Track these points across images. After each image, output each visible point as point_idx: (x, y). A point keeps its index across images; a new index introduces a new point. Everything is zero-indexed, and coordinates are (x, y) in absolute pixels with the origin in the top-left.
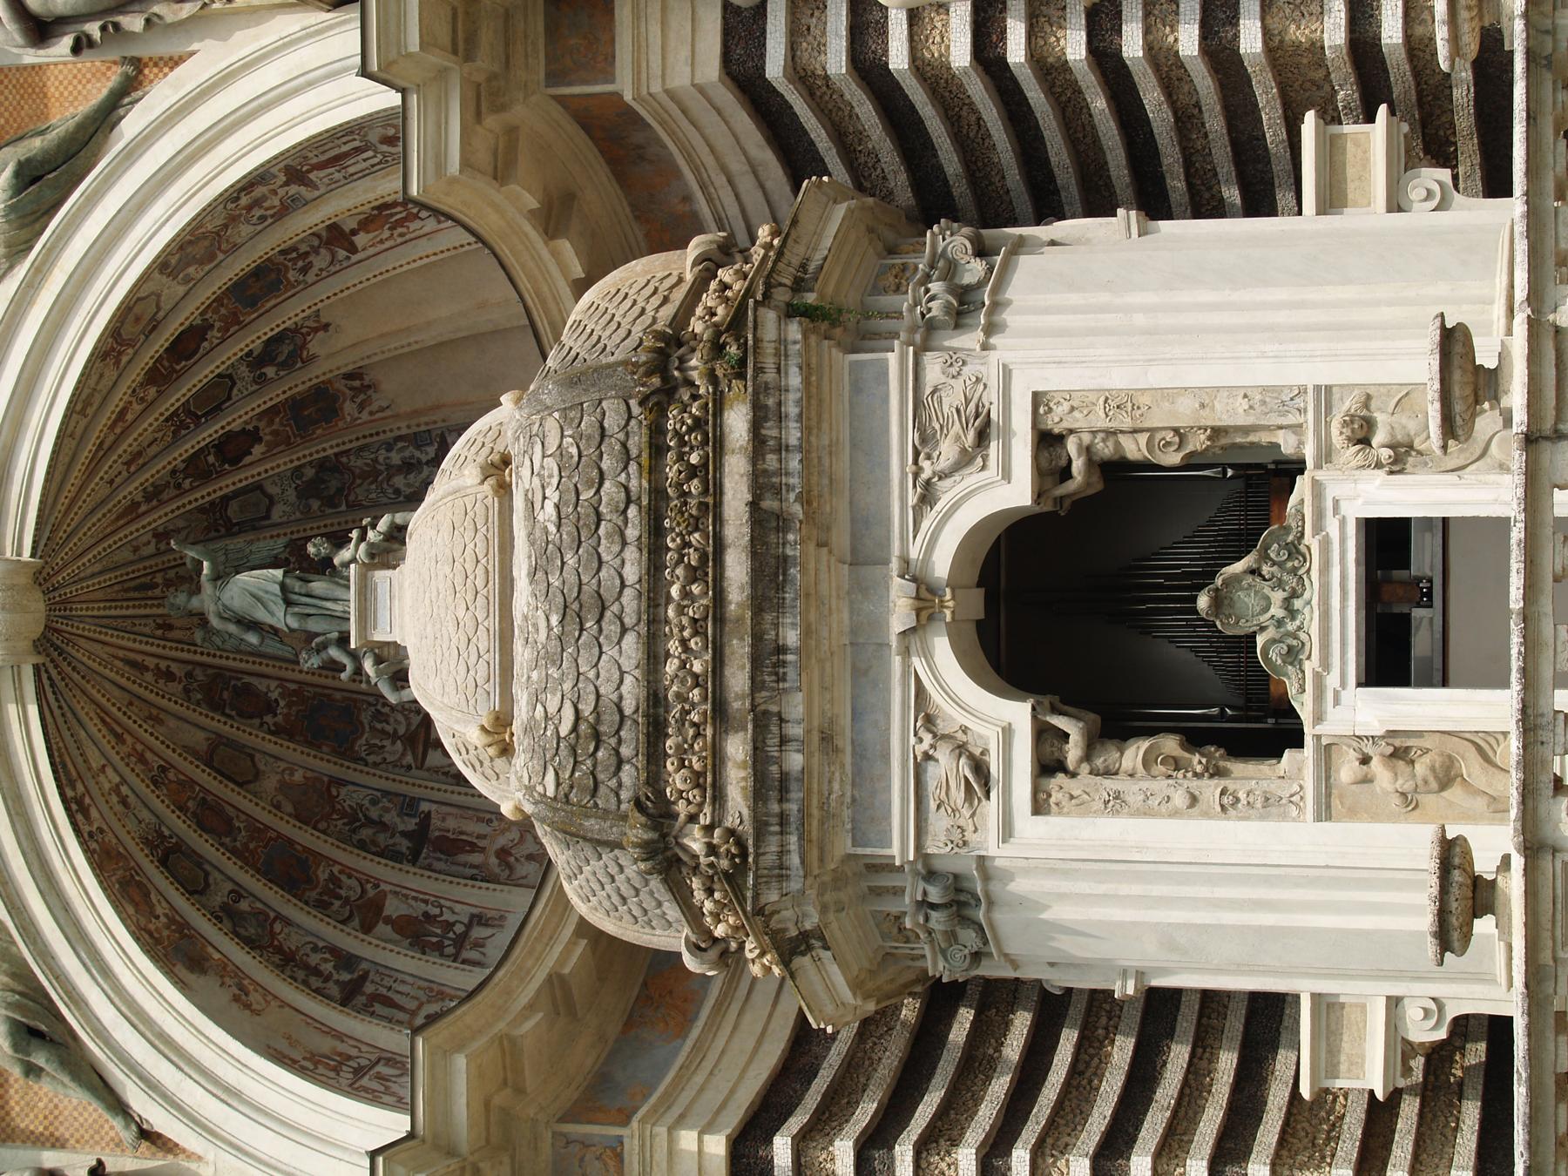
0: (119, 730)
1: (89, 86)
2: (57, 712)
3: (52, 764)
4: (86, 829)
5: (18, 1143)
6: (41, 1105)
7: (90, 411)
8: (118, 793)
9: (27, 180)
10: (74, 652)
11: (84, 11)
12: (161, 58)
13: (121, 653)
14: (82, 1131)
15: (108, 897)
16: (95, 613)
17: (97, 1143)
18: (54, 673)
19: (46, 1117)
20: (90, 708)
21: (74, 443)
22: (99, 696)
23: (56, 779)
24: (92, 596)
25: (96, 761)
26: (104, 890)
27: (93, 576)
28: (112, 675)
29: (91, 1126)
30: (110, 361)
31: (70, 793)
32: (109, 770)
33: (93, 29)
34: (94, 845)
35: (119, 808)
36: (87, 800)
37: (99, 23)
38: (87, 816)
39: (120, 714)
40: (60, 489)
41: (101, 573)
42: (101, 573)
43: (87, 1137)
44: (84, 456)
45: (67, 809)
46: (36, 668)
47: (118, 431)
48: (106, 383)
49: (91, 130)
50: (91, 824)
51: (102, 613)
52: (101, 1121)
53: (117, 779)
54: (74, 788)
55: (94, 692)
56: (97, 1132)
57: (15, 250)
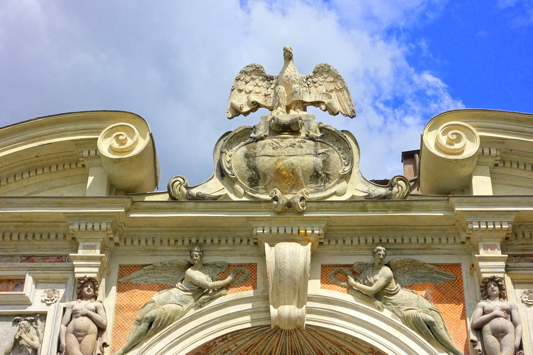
0: (249, 350)
2: (255, 332)
3: (238, 331)
4: (217, 341)
5: (114, 316)
6: (127, 324)
7: (354, 343)
8: (228, 350)
9: (429, 325)
10: (275, 336)
11: (485, 344)
13: (274, 350)
14: (118, 338)
15: (195, 349)
16: (287, 343)
17: (114, 343)
18: (268, 330)
19: (123, 326)
20: (256, 341)
21: (343, 338)
22: (260, 344)
23: (233, 332)
24: (293, 341)
25: (239, 343)
26: (197, 348)
27: (300, 342)
28: (267, 348)
29: (119, 341)
30: (370, 350)
31: (228, 336)
32: (236, 347)
33: (479, 347)
34: (211, 344)
35: (223, 351)
36: (226, 341)
37: (481, 349)
38: (221, 341)
39: (254, 350)
40: (328, 333)
41: (301, 344)
42: (301, 344)
43: (116, 340)
44: (339, 341)
45: (224, 335)
46: (270, 326)
47: (347, 351)
48: (363, 349)
49: (446, 345)
50: (218, 342)
51: (287, 345)
52: (121, 345)
53: (233, 350)
54: (230, 337)
55: (261, 343)
56: (117, 343)
57: (406, 319)
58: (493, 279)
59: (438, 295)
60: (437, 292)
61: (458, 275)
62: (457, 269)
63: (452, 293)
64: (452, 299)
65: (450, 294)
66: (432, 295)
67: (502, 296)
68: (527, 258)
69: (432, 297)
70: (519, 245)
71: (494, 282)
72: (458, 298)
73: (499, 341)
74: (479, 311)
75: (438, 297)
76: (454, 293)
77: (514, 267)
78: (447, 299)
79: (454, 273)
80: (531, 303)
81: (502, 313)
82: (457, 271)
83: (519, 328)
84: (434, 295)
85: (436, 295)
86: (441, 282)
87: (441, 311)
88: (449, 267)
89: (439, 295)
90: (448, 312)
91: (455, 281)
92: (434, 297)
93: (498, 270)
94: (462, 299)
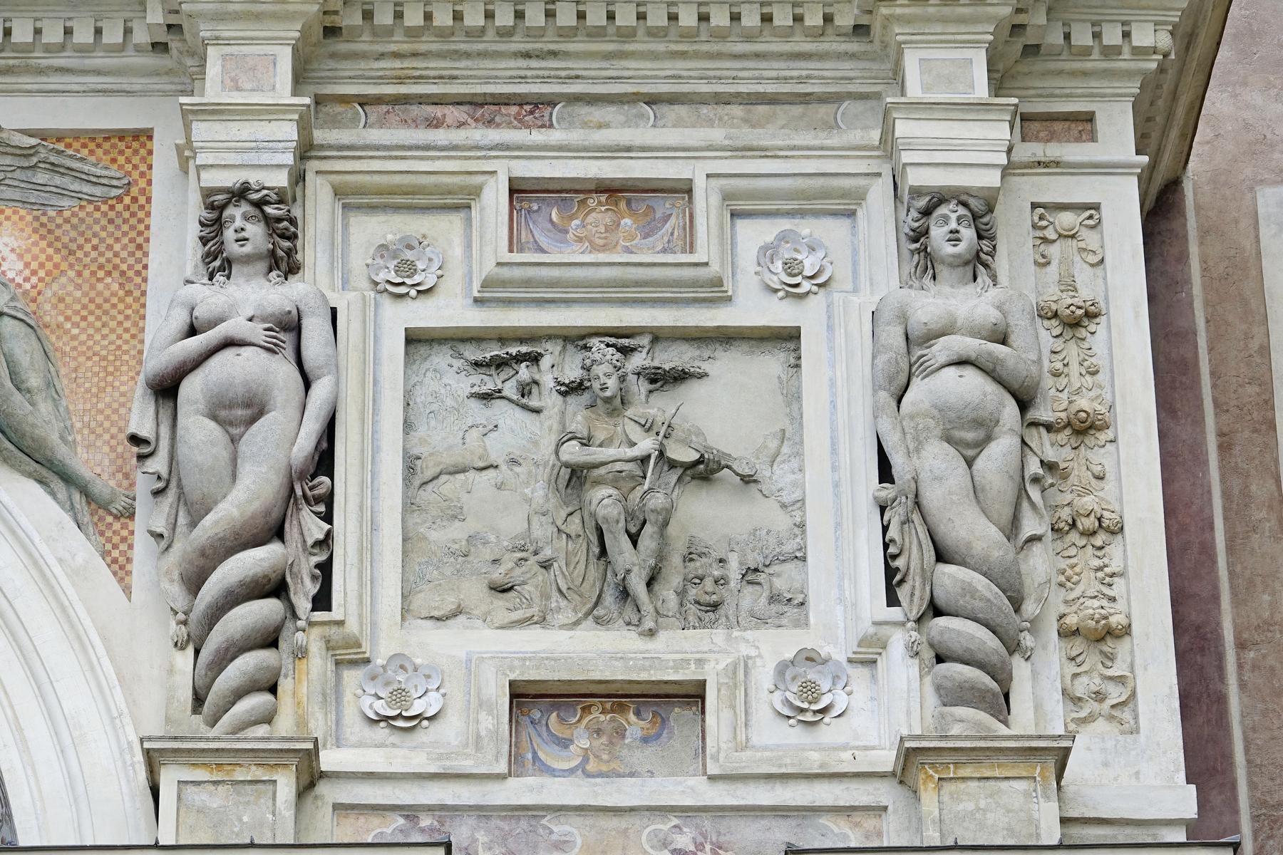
1: (106, 449)
12: (131, 547)
33: (158, 464)
58: (240, 193)
59: (43, 257)
60: (43, 244)
61: (136, 174)
62: (136, 152)
63: (102, 248)
64: (101, 274)
65: (94, 254)
66: (20, 257)
67: (283, 262)
68: (415, 110)
69: (20, 266)
70: (382, 56)
71: (245, 207)
72: (124, 267)
73: (234, 440)
74: (179, 320)
75: (42, 265)
76: (110, 247)
77: (350, 148)
78: (79, 274)
79: (121, 167)
80: (402, 290)
81: (257, 332)
82: (136, 160)
83: (321, 390)
84: (28, 258)
85: (35, 258)
86: (66, 203)
87: (47, 319)
88: (107, 145)
89: (49, 258)
90: (76, 325)
91: (119, 199)
92: (27, 265)
93: (266, 158)
94: (138, 273)
